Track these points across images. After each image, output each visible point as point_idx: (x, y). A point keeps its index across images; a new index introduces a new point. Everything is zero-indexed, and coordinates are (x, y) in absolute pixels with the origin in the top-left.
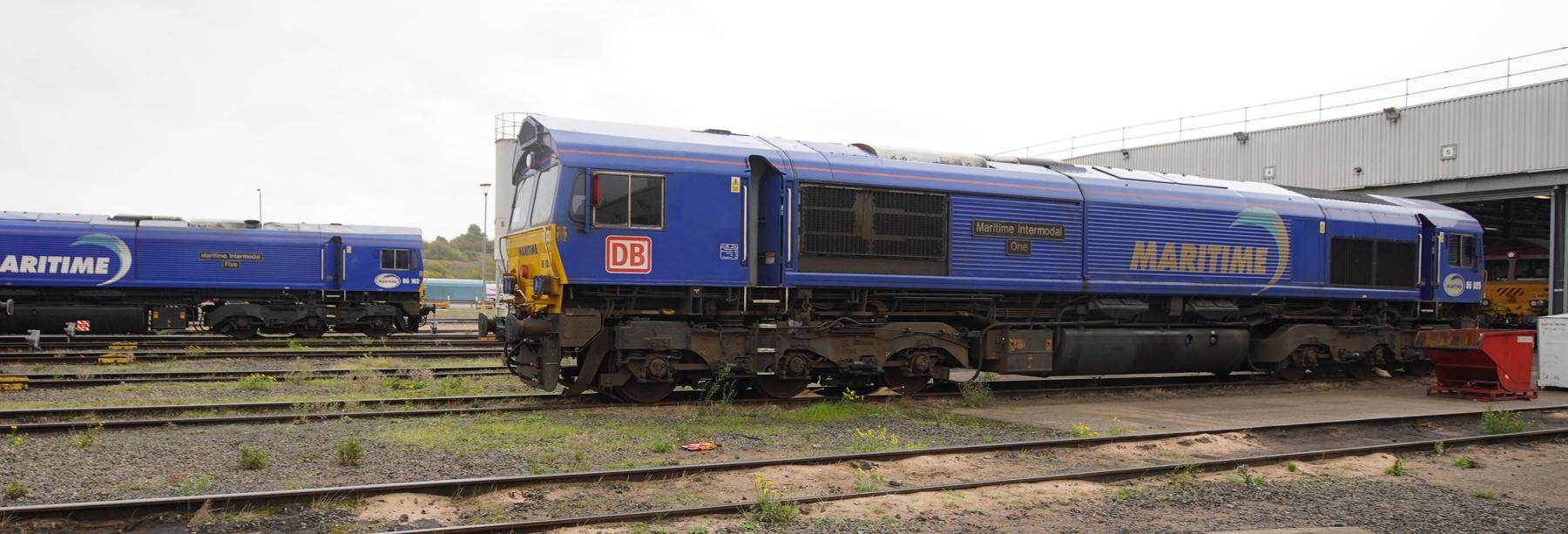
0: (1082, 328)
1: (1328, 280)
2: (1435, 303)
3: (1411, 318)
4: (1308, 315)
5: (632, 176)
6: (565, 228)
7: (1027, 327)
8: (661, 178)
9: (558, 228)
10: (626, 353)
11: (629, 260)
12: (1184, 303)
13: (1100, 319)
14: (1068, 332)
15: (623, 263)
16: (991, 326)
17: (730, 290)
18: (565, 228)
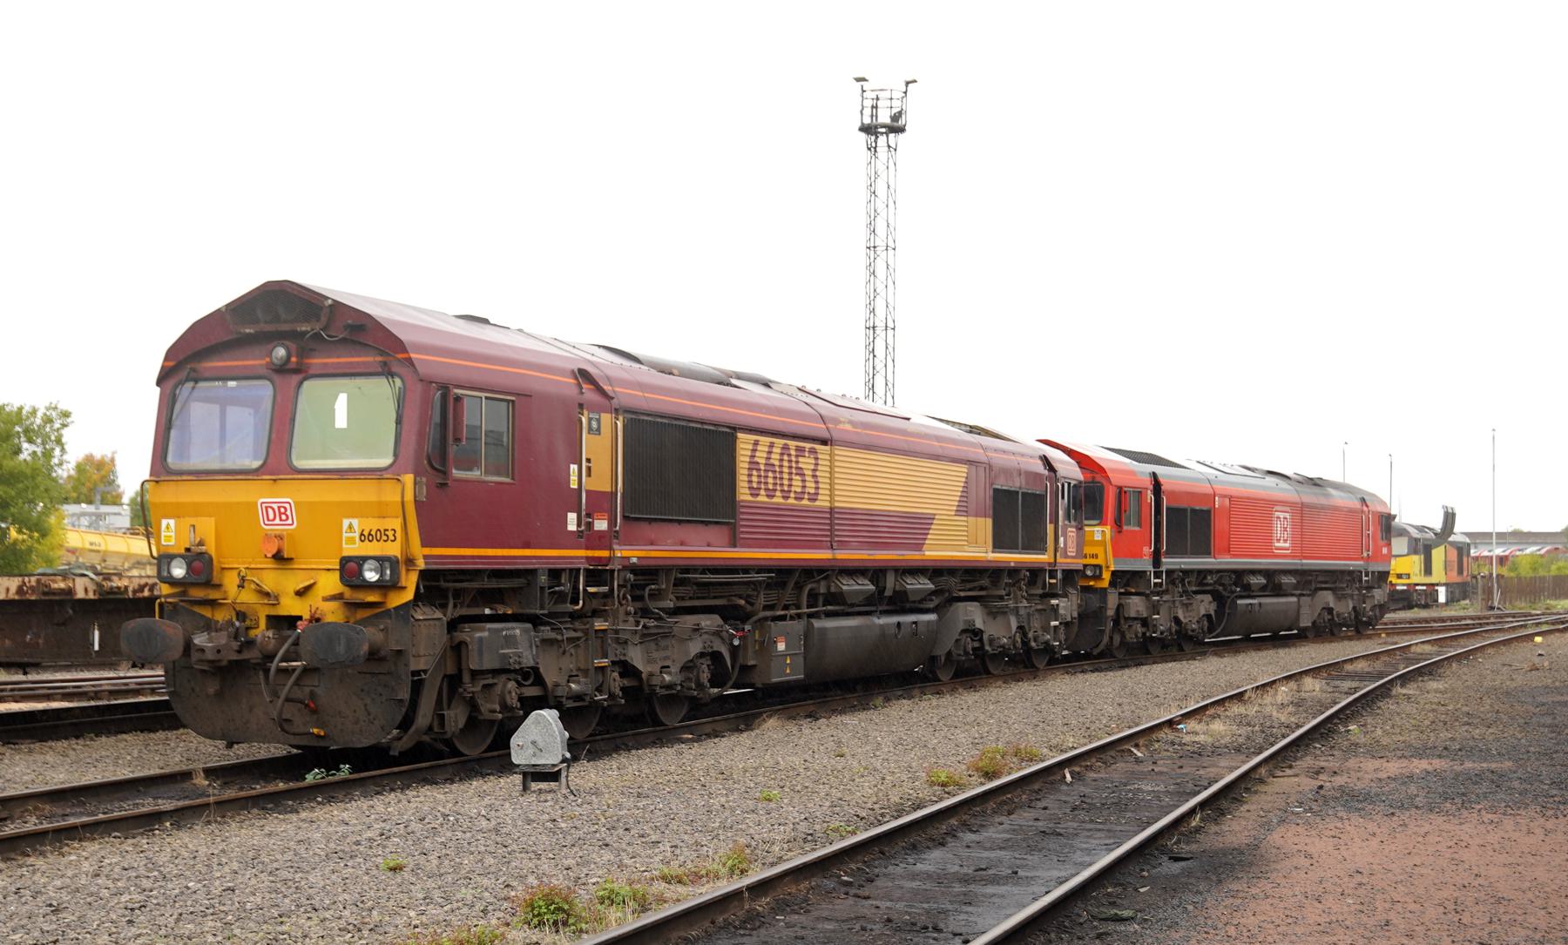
0: (823, 616)
1: (991, 548)
2: (1057, 570)
3: (1040, 591)
4: (970, 590)
5: (486, 398)
6: (424, 479)
7: (783, 618)
8: (508, 401)
9: (418, 479)
10: (475, 674)
11: (278, 518)
12: (896, 580)
13: (839, 605)
14: (817, 624)
15: (274, 519)
16: (755, 618)
17: (568, 571)
18: (424, 479)
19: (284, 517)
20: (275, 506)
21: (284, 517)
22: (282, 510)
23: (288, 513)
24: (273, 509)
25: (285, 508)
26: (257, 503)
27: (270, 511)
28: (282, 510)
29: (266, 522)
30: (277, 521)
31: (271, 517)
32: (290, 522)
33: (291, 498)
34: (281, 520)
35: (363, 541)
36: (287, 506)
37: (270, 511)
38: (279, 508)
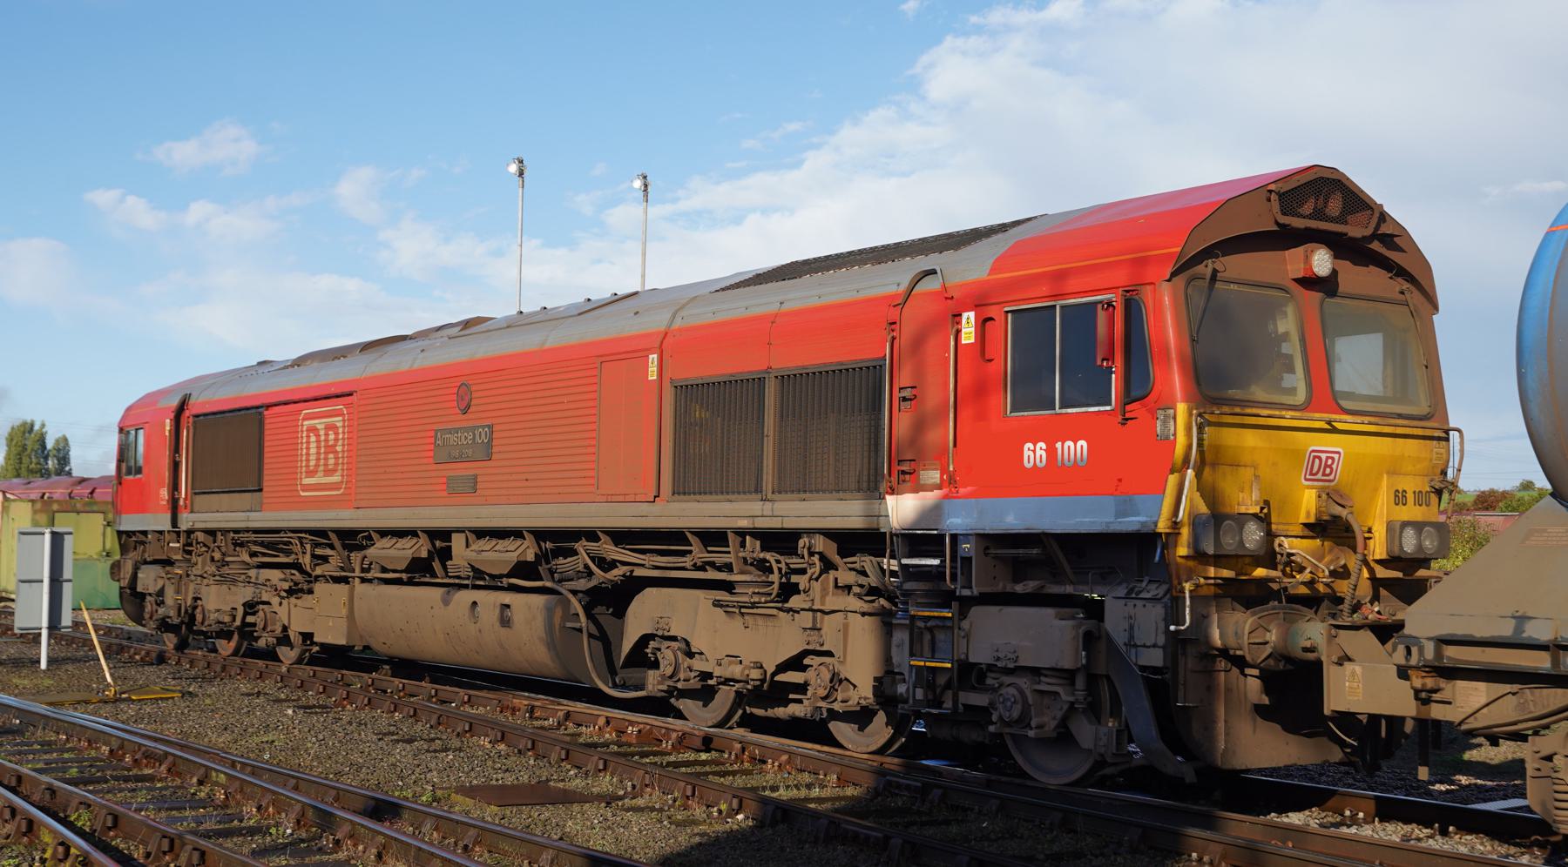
19: (1328, 471)
20: (1323, 456)
21: (1328, 471)
22: (1330, 462)
23: (1334, 466)
24: (1320, 458)
25: (1333, 459)
26: (1307, 450)
27: (1317, 461)
28: (1330, 462)
29: (1308, 477)
30: (1319, 476)
31: (1314, 472)
32: (1331, 477)
33: (1341, 447)
34: (1324, 474)
35: (1397, 504)
36: (1336, 456)
37: (1317, 461)
38: (1328, 458)
